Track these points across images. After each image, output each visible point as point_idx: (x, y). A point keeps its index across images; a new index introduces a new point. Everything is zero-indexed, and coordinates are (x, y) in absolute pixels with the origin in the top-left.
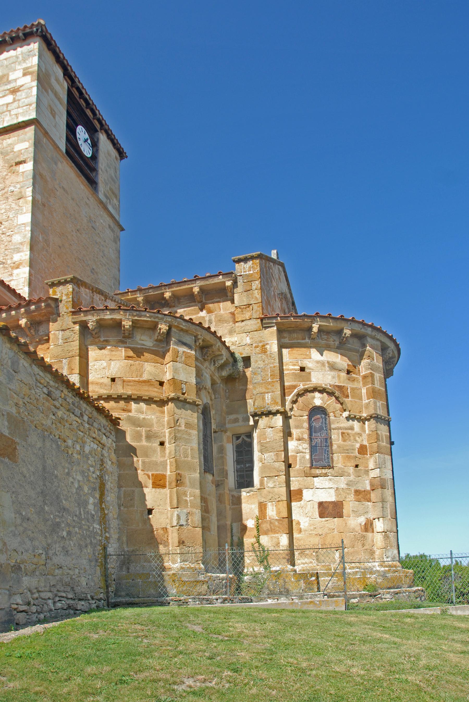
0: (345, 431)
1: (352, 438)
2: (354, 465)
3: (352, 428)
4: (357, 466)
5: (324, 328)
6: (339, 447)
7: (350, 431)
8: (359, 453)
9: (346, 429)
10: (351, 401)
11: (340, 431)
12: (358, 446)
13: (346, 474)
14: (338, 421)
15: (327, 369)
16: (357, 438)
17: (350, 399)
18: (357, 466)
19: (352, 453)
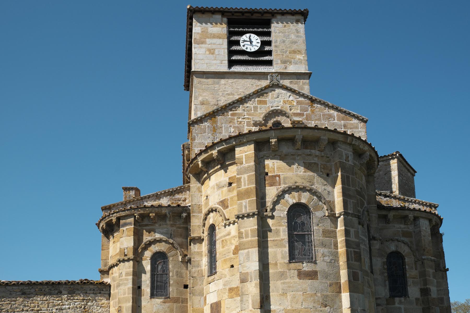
0: (223, 239)
1: (229, 242)
2: (229, 266)
3: (229, 234)
4: (232, 266)
5: (207, 160)
6: (220, 254)
7: (227, 237)
8: (234, 254)
9: (225, 236)
10: (230, 210)
11: (221, 240)
12: (233, 247)
13: (223, 276)
14: (220, 233)
15: (216, 190)
16: (233, 241)
17: (229, 208)
18: (232, 266)
19: (228, 256)
